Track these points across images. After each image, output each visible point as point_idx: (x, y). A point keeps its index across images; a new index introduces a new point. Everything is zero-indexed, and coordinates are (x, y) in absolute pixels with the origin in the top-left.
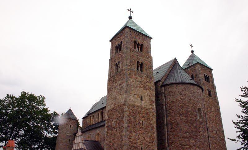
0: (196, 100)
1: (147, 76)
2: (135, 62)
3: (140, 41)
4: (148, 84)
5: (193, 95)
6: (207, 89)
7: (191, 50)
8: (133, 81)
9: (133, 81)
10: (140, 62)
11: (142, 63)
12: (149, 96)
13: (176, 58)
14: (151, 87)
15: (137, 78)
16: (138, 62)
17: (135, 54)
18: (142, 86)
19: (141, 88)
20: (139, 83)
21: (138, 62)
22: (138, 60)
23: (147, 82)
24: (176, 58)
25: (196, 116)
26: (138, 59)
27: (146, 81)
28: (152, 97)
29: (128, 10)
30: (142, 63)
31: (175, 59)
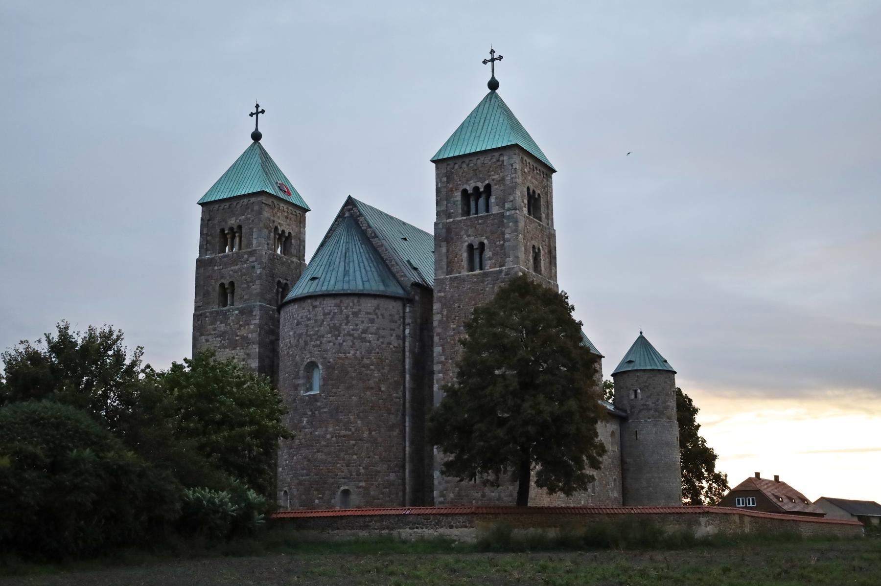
0: (302, 342)
1: (242, 312)
2: (214, 290)
3: (233, 222)
4: (243, 332)
5: (295, 333)
6: (466, 244)
7: (489, 78)
8: (207, 341)
9: (207, 341)
10: (226, 282)
11: (232, 284)
12: (244, 360)
13: (350, 196)
14: (250, 336)
15: (214, 330)
16: (222, 285)
17: (216, 268)
18: (226, 343)
19: (225, 348)
20: (219, 339)
21: (222, 285)
22: (223, 281)
23: (241, 326)
24: (350, 196)
25: (296, 389)
26: (222, 277)
27: (236, 326)
28: (249, 361)
29: (257, 106)
30: (232, 284)
31: (350, 202)
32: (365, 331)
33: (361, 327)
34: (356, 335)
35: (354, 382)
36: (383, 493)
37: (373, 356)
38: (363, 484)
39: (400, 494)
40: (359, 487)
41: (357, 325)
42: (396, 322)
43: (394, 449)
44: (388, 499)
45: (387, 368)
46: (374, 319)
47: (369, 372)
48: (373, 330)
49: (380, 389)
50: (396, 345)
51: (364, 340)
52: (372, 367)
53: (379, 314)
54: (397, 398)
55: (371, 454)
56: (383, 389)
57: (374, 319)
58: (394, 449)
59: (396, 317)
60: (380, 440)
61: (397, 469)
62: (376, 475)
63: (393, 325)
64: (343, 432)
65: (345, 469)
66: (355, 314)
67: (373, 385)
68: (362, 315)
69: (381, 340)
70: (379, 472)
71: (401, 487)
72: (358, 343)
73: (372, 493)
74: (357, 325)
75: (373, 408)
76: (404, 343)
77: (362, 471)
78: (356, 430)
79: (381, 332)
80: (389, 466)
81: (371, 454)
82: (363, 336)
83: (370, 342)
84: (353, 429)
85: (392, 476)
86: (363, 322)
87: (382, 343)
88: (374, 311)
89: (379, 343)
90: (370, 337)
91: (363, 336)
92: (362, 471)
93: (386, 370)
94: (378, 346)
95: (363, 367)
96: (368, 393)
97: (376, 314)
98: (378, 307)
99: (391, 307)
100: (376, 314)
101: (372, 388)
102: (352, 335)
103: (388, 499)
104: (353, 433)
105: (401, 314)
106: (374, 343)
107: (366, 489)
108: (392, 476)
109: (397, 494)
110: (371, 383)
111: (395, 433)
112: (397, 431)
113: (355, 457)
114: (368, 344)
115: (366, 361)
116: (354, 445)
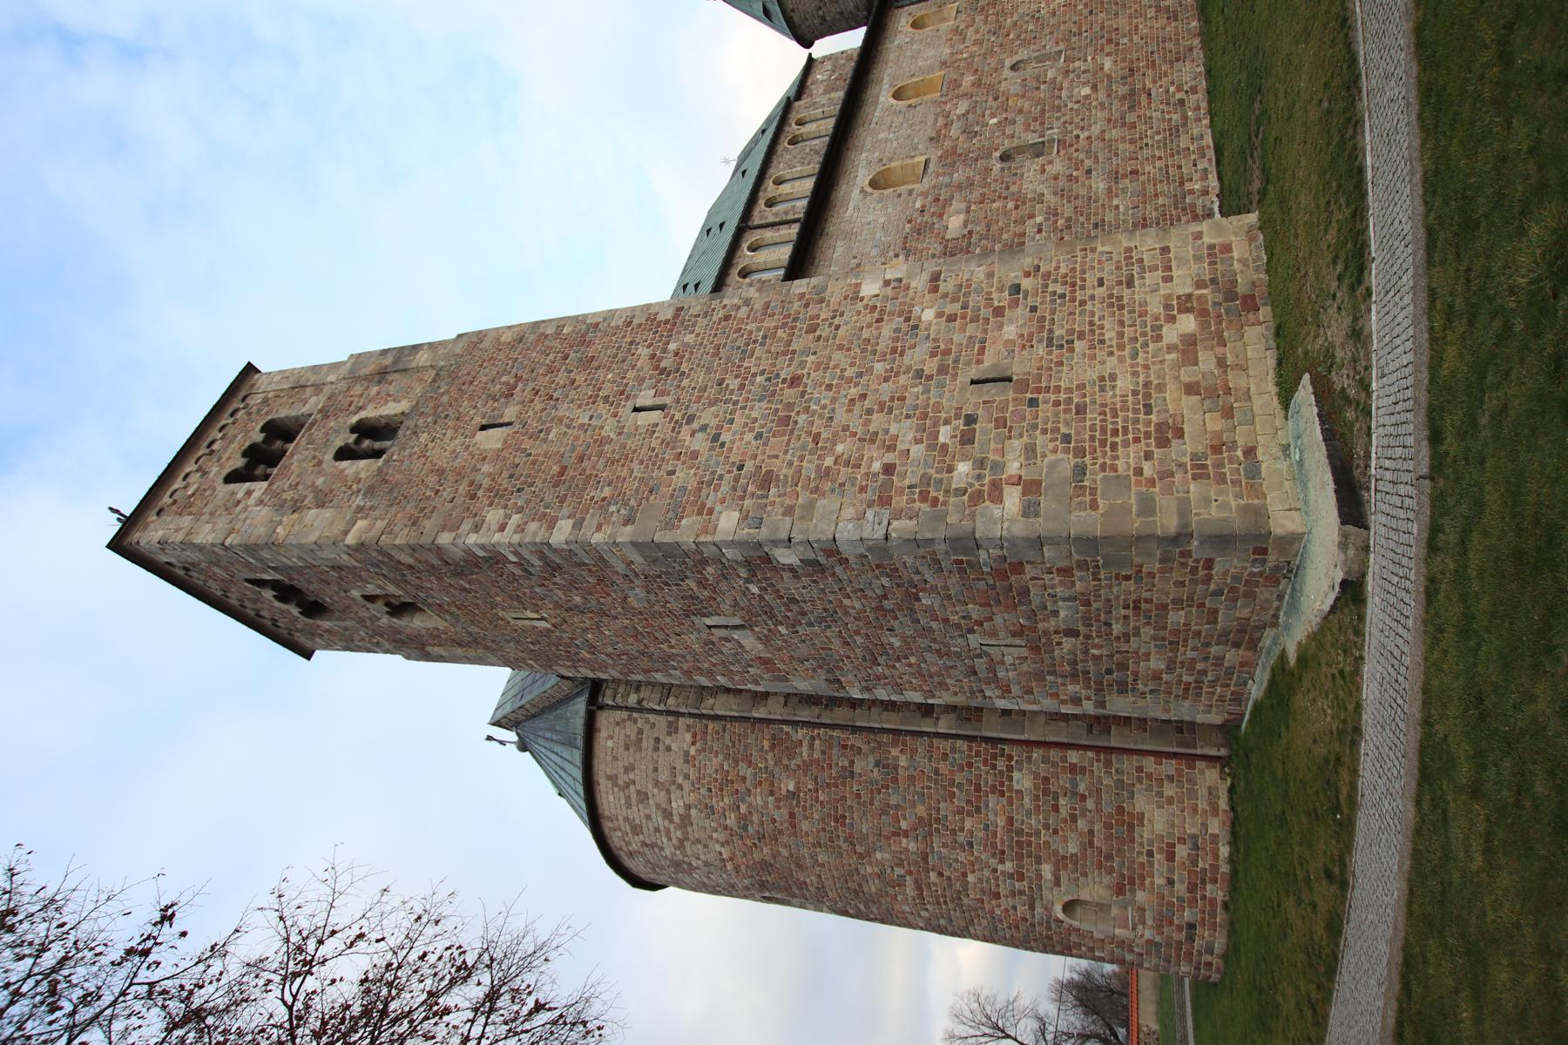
32: (668, 815)
33: (659, 820)
34: (679, 834)
35: (785, 853)
36: (1074, 819)
37: (719, 805)
38: (1047, 870)
39: (1073, 757)
40: (1057, 882)
41: (657, 830)
42: (640, 732)
43: (944, 768)
44: (1090, 804)
45: (743, 769)
46: (638, 792)
47: (755, 818)
48: (660, 797)
49: (793, 795)
50: (688, 737)
51: (686, 820)
52: (743, 809)
53: (626, 778)
54: (811, 746)
55: (961, 838)
56: (791, 788)
57: (638, 792)
58: (944, 768)
59: (631, 730)
60: (921, 810)
61: (1001, 764)
62: (1020, 832)
63: (647, 743)
64: (910, 890)
65: (1006, 903)
66: (636, 829)
67: (785, 811)
68: (637, 814)
69: (680, 780)
70: (1010, 820)
71: (1054, 754)
72: (695, 833)
73: (1073, 848)
74: (657, 830)
75: (840, 820)
76: (683, 715)
77: (1009, 866)
78: (900, 865)
79: (664, 776)
80: (993, 789)
81: (961, 838)
82: (676, 819)
83: (688, 807)
84: (899, 871)
85: (1023, 781)
86: (648, 817)
87: (686, 777)
88: (622, 789)
89: (687, 786)
90: (677, 805)
91: (676, 819)
92: (1009, 866)
93: (749, 773)
94: (694, 790)
95: (745, 828)
96: (805, 826)
97: (627, 785)
98: (613, 778)
99: (610, 743)
100: (627, 785)
101: (792, 815)
102: (681, 841)
103: (1090, 804)
104: (910, 873)
105: (625, 714)
106: (692, 798)
107: (1060, 862)
108: (1023, 781)
109: (1073, 768)
110: (781, 815)
111: (903, 762)
112: (895, 752)
113: (971, 878)
114: (693, 812)
115: (731, 820)
116: (940, 874)
